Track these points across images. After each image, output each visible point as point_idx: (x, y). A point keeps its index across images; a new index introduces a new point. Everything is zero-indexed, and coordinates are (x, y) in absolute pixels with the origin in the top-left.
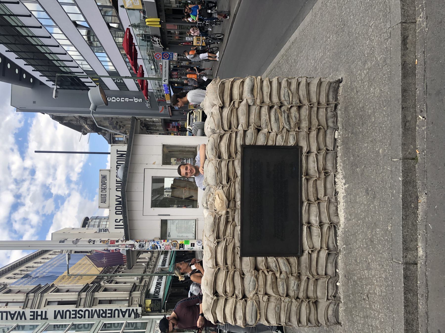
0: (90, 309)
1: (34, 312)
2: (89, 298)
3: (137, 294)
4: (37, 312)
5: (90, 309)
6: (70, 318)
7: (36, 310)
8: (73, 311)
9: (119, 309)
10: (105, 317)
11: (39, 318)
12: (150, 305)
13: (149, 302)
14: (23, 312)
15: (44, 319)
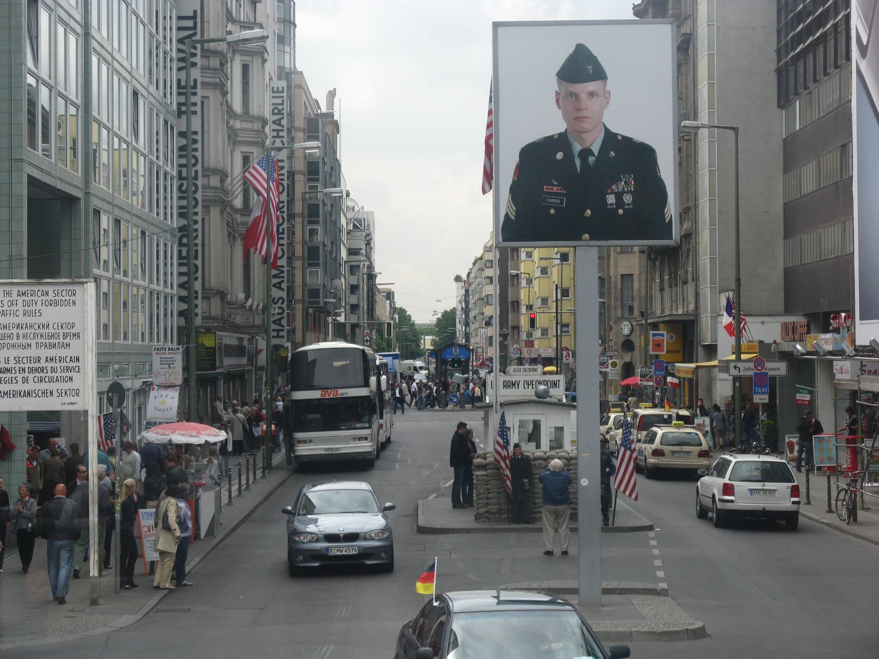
0: (199, 209)
1: (195, 87)
2: (210, 194)
3: (216, 307)
4: (195, 94)
5: (199, 209)
6: (181, 166)
7: (199, 90)
8: (196, 172)
9: (199, 274)
10: (181, 244)
11: (182, 99)
12: (203, 344)
13: (208, 342)
14: (194, 64)
15: (179, 109)
